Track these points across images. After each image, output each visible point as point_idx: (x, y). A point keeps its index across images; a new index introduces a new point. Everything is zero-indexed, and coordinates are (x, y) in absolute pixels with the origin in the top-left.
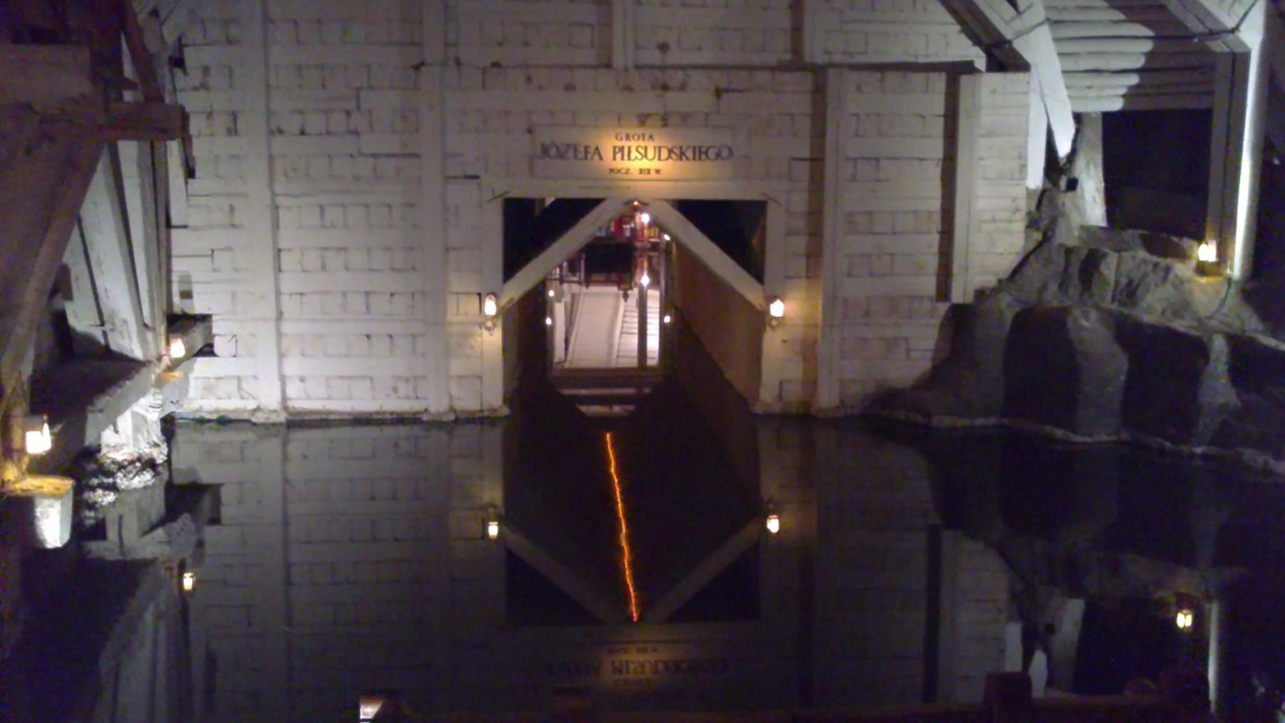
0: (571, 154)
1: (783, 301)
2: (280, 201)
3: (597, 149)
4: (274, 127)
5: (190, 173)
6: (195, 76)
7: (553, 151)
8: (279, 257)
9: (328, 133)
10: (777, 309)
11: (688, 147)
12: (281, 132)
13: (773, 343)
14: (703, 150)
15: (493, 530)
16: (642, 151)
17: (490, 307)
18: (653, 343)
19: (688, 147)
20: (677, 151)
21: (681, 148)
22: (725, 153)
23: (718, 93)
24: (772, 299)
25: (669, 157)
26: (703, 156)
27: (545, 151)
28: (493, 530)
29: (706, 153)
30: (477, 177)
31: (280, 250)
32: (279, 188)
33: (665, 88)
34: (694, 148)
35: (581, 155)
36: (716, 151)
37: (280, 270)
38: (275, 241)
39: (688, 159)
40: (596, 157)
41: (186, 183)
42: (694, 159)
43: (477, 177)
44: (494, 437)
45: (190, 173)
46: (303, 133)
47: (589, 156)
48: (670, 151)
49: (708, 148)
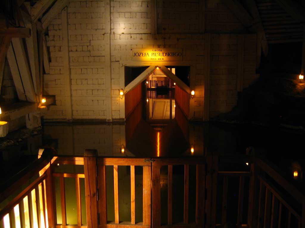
0: (142, 55)
1: (194, 91)
2: (72, 67)
3: (148, 53)
4: (70, 50)
5: (50, 61)
6: (51, 38)
7: (137, 54)
8: (71, 81)
9: (83, 51)
10: (193, 93)
11: (170, 53)
12: (71, 51)
13: (192, 101)
14: (174, 53)
15: (123, 150)
16: (159, 54)
17: (122, 93)
18: (174, 113)
19: (170, 53)
20: (168, 54)
21: (169, 53)
22: (180, 54)
23: (178, 39)
24: (191, 91)
25: (166, 55)
26: (174, 55)
27: (135, 54)
28: (123, 150)
29: (175, 54)
30: (119, 61)
31: (71, 79)
32: (71, 64)
33: (165, 38)
34: (172, 53)
35: (144, 55)
36: (178, 54)
37: (71, 84)
38: (70, 77)
39: (170, 56)
40: (148, 55)
41: (49, 63)
42: (172, 56)
43: (119, 61)
44: (123, 128)
45: (50, 61)
46: (77, 51)
47: (146, 55)
48: (166, 54)
49: (176, 53)
